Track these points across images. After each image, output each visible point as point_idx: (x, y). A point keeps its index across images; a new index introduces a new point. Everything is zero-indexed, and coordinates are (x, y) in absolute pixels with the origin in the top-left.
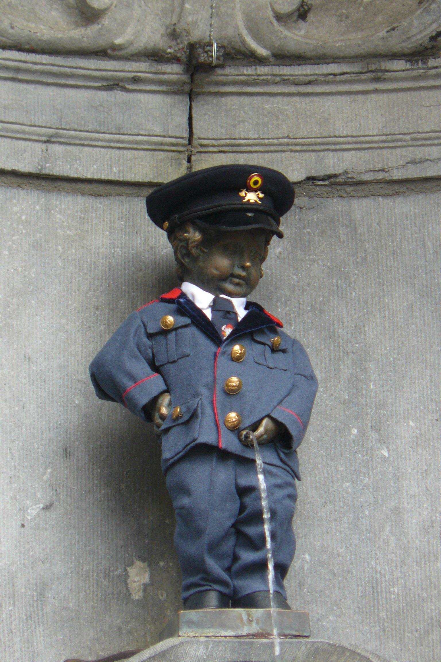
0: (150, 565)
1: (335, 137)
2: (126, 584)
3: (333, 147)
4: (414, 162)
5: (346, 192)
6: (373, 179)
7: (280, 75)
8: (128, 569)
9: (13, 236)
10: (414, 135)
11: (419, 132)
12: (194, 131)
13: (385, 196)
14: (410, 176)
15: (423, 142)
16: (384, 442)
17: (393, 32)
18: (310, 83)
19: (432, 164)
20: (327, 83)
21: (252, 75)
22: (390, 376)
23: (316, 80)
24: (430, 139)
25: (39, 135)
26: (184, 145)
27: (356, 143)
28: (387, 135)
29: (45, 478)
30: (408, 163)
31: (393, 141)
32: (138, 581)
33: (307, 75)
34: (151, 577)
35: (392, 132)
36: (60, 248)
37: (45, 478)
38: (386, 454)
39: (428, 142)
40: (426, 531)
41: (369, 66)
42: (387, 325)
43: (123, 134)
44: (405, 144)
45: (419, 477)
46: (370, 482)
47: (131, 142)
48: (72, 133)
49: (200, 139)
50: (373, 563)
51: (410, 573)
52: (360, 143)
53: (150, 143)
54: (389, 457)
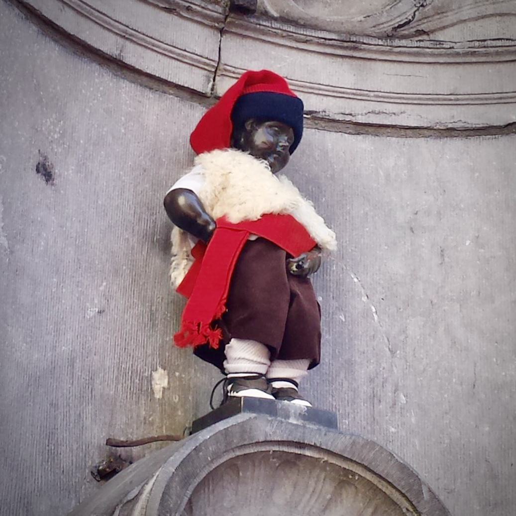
0: (168, 375)
1: (320, 84)
2: (151, 385)
3: (317, 92)
5: (322, 126)
7: (288, 31)
8: (153, 373)
9: (94, 100)
12: (222, 58)
14: (371, 122)
15: (382, 99)
16: (342, 310)
17: (368, 18)
18: (306, 42)
19: (388, 116)
20: (319, 44)
21: (268, 27)
22: (348, 262)
23: (312, 40)
24: (388, 97)
25: (119, 29)
26: (213, 66)
27: (333, 92)
30: (369, 113)
32: (159, 384)
34: (169, 383)
36: (123, 118)
37: (102, 288)
38: (344, 320)
39: (385, 100)
40: (372, 380)
41: (351, 37)
43: (175, 47)
44: (369, 99)
45: (368, 338)
46: (330, 338)
47: (179, 55)
48: (142, 36)
49: (226, 65)
50: (331, 400)
51: (359, 411)
52: (336, 92)
54: (345, 322)
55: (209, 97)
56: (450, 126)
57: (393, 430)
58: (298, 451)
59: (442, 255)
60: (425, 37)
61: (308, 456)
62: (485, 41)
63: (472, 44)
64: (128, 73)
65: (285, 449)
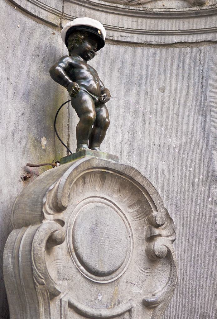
0: (47, 139)
2: (41, 143)
4: (121, 36)
6: (109, 38)
10: (123, 28)
11: (124, 28)
13: (112, 44)
23: (98, 5)
26: (61, 14)
28: (115, 26)
29: (22, 105)
31: (116, 29)
33: (96, 3)
35: (117, 26)
37: (22, 105)
40: (120, 143)
42: (111, 81)
43: (46, 5)
44: (119, 30)
47: (48, 9)
49: (65, 14)
53: (52, 10)
55: (59, 27)
56: (151, 43)
57: (129, 162)
58: (106, 171)
59: (148, 95)
60: (141, 6)
61: (110, 173)
62: (165, 9)
63: (160, 10)
64: (29, 15)
65: (103, 170)
